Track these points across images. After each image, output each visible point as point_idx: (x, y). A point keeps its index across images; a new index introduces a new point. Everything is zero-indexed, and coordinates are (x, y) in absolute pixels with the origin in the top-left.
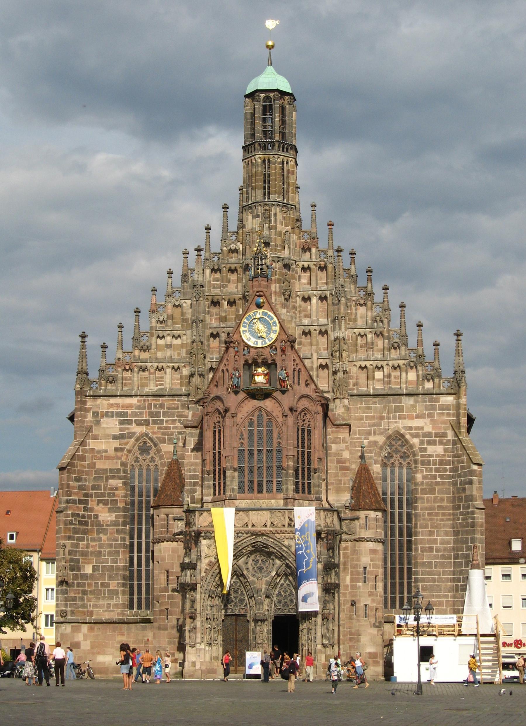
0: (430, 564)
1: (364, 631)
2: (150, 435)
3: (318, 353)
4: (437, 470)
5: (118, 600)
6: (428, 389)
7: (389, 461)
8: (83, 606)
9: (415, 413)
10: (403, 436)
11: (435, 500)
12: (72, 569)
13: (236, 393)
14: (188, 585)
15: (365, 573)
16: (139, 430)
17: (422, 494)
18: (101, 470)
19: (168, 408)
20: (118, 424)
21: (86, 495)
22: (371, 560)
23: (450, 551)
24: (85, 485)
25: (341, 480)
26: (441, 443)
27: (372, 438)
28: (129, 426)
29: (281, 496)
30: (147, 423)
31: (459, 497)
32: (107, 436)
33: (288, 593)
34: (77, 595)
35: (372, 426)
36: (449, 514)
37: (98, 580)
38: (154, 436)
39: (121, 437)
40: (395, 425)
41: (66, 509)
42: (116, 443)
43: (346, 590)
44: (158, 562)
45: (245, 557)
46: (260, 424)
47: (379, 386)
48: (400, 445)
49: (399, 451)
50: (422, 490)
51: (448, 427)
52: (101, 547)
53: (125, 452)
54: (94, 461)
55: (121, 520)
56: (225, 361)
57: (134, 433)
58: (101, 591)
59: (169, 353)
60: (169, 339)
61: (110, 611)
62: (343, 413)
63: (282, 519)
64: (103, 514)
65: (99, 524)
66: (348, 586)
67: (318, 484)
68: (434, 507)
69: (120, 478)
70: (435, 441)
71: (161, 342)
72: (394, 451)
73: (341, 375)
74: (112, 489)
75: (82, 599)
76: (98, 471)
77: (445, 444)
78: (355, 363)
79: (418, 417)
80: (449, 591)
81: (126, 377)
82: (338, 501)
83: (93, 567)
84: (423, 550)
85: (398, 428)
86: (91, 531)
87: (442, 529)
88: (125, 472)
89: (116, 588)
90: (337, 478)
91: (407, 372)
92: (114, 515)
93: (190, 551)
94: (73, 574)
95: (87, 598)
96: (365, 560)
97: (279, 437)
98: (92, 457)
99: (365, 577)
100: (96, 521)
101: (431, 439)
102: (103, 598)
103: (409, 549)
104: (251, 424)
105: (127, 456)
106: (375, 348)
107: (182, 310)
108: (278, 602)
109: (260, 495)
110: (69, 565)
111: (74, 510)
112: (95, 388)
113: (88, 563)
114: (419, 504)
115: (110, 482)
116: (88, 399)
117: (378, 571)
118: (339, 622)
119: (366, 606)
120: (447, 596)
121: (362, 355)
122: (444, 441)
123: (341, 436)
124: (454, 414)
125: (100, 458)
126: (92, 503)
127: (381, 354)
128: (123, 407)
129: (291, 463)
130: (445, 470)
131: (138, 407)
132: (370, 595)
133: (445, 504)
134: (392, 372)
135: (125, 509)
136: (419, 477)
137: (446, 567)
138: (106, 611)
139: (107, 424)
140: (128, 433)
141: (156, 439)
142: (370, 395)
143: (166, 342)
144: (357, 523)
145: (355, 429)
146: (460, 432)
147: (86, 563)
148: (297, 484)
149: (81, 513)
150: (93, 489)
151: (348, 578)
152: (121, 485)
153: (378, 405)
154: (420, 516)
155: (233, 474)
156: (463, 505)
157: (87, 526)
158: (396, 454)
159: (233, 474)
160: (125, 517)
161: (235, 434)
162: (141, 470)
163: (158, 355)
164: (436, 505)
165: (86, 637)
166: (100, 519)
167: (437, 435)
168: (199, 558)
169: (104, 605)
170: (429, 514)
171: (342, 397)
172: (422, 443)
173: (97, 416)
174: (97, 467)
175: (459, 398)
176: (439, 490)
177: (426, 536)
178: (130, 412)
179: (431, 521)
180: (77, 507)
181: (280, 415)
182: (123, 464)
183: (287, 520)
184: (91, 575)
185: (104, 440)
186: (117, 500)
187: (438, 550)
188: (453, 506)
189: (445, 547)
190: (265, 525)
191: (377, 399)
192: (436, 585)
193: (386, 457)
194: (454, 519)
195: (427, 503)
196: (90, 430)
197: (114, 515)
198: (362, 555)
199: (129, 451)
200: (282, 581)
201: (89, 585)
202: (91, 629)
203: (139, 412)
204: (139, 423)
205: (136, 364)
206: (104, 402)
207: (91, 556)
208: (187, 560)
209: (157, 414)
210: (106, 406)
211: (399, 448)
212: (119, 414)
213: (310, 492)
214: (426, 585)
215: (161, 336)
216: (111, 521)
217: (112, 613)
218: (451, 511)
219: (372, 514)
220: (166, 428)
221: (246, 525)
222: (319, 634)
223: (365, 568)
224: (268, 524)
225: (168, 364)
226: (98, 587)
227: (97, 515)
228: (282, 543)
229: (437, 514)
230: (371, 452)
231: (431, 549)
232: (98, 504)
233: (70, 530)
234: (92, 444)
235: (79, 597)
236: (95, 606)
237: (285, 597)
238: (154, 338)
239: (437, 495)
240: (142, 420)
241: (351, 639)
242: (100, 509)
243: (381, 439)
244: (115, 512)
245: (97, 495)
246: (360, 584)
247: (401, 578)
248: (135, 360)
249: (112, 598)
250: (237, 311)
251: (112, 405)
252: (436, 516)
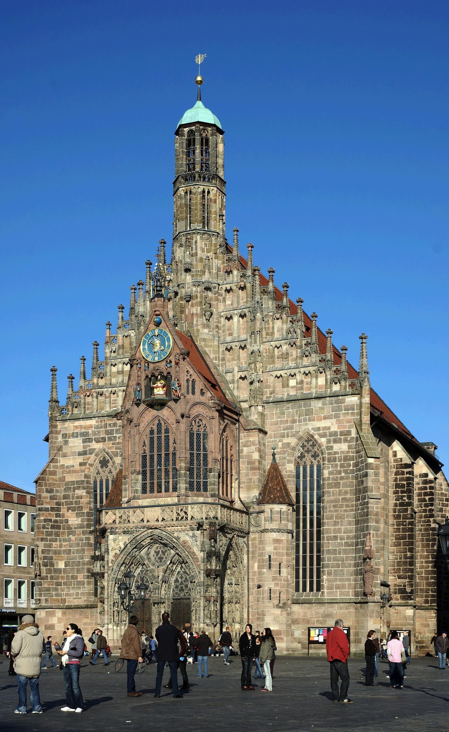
0: (335, 552)
1: (268, 611)
2: (107, 450)
3: (239, 367)
4: (342, 466)
5: (84, 589)
6: (336, 392)
7: (301, 460)
8: (57, 595)
9: (323, 415)
10: (312, 436)
11: (340, 493)
12: (45, 565)
13: (138, 405)
14: (98, 574)
15: (270, 561)
17: (328, 488)
18: (69, 482)
20: (81, 442)
21: (58, 504)
22: (275, 549)
23: (352, 538)
24: (56, 496)
25: (251, 479)
26: (346, 441)
27: (286, 440)
28: (90, 444)
29: (176, 493)
30: (104, 440)
31: (359, 489)
32: (73, 454)
33: (184, 579)
34: (50, 586)
35: (286, 429)
36: (352, 506)
37: (69, 573)
38: (109, 451)
40: (305, 427)
41: (38, 515)
42: (80, 459)
43: (254, 576)
45: (146, 549)
46: (159, 432)
47: (293, 393)
48: (311, 446)
49: (310, 451)
50: (328, 484)
51: (352, 425)
52: (70, 547)
53: (87, 466)
54: (64, 475)
55: (85, 523)
57: (94, 449)
58: (71, 582)
59: (120, 378)
61: (79, 598)
62: (256, 419)
63: (171, 513)
64: (72, 519)
65: (69, 528)
66: (256, 572)
67: (213, 482)
68: (339, 499)
69: (84, 488)
70: (340, 439)
71: (114, 369)
72: (306, 451)
73: (256, 384)
74: (78, 497)
75: (56, 590)
76: (67, 484)
77: (349, 442)
78: (272, 373)
79: (325, 418)
80: (351, 575)
81: (89, 402)
82: (248, 498)
83: (65, 562)
84: (329, 539)
85: (308, 429)
86: (63, 533)
87: (346, 520)
88: (88, 482)
89: (83, 580)
90: (247, 477)
91: (317, 378)
92: (80, 520)
93: (100, 545)
94: (46, 570)
95: (61, 589)
96: (269, 549)
97: (175, 442)
98: (63, 472)
99: (270, 564)
100: (67, 525)
101: (336, 437)
102: (73, 588)
103: (319, 538)
104: (152, 432)
105: (90, 469)
106: (290, 358)
107: (130, 339)
108: (176, 588)
109: (159, 494)
110: (43, 562)
111: (46, 516)
112: (64, 413)
113: (61, 560)
114: (326, 498)
115: (76, 491)
116: (58, 423)
117: (282, 559)
118: (248, 604)
119: (270, 590)
120: (349, 580)
121: (278, 365)
122: (349, 439)
123: (251, 439)
124: (357, 413)
125: (68, 473)
126: (64, 510)
127: (295, 363)
128: (85, 428)
129: (183, 465)
130: (349, 465)
131: (97, 427)
132: (273, 580)
133: (348, 496)
134: (305, 378)
135: (88, 514)
136: (326, 473)
137: (349, 553)
138: (75, 598)
139: (73, 443)
140: (90, 450)
141: (111, 454)
142: (284, 401)
143: (118, 369)
144: (262, 516)
145: (271, 433)
146: (361, 429)
147: (59, 560)
148: (191, 484)
149: (54, 518)
150: (63, 499)
151: (256, 565)
152: (85, 494)
153: (290, 410)
154: (327, 508)
155: (137, 477)
156: (362, 496)
157: (60, 529)
158: (308, 454)
159: (137, 477)
160: (88, 520)
161: (138, 441)
162: (101, 482)
163: (112, 381)
164: (341, 497)
165: (60, 620)
166: (70, 523)
167: (342, 434)
168: (107, 551)
169: (74, 593)
170: (334, 506)
171: (256, 404)
172: (329, 441)
173: (65, 437)
174: (66, 480)
175: (361, 397)
176: (343, 483)
177: (331, 526)
178: (90, 431)
179: (336, 512)
180: (50, 514)
181: (175, 422)
182: (86, 476)
183: (175, 515)
184: (64, 569)
185: (71, 457)
186: (82, 507)
187: (342, 539)
188: (356, 497)
189: (348, 536)
190: (157, 520)
191: (291, 404)
192: (340, 570)
193: (299, 457)
194: (356, 509)
195: (333, 496)
196: (60, 449)
198: (267, 544)
199: (91, 465)
200: (179, 569)
201: (62, 578)
202: (64, 614)
203: (97, 431)
204: (98, 441)
205: (94, 390)
206: (71, 425)
207: (64, 554)
208: (97, 553)
209: (111, 432)
210: (72, 428)
211: (311, 448)
212: (82, 434)
213: (206, 490)
214: (331, 570)
216: (78, 525)
217: (80, 600)
218: (354, 503)
219: (277, 507)
221: (142, 520)
222: (202, 614)
223: (270, 556)
224: (160, 519)
225: (120, 388)
226: (69, 579)
227: (68, 520)
228: (172, 535)
229: (341, 506)
230: (284, 452)
231: (336, 538)
232: (68, 511)
233: (42, 533)
234: (62, 461)
235: (53, 588)
236: (67, 595)
237: (182, 583)
238: (109, 367)
239: (341, 488)
240: (100, 438)
241: (258, 619)
242: (70, 514)
243: (293, 441)
244: (80, 516)
245: (67, 504)
246: (265, 570)
247: (311, 564)
248: (94, 387)
249: (79, 588)
251: (76, 426)
252: (340, 508)
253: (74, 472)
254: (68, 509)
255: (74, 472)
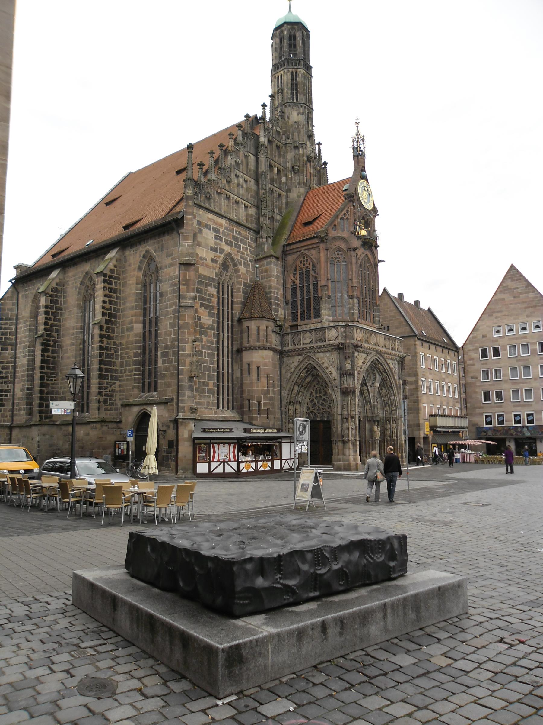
16: (227, 248)
19: (243, 237)
32: (206, 246)
37: (201, 379)
39: (214, 250)
44: (258, 368)
52: (202, 348)
56: (344, 211)
57: (223, 250)
60: (241, 180)
65: (201, 327)
76: (201, 276)
89: (213, 388)
128: (217, 224)
131: (226, 228)
138: (206, 408)
140: (220, 249)
152: (216, 293)
166: (202, 321)
186: (213, 306)
197: (211, 319)
215: (238, 174)
216: (210, 325)
220: (243, 253)
225: (243, 201)
227: (200, 317)
232: (200, 307)
244: (212, 316)
249: (210, 397)
250: (281, 178)
253: (207, 266)
254: (201, 305)
255: (207, 266)
